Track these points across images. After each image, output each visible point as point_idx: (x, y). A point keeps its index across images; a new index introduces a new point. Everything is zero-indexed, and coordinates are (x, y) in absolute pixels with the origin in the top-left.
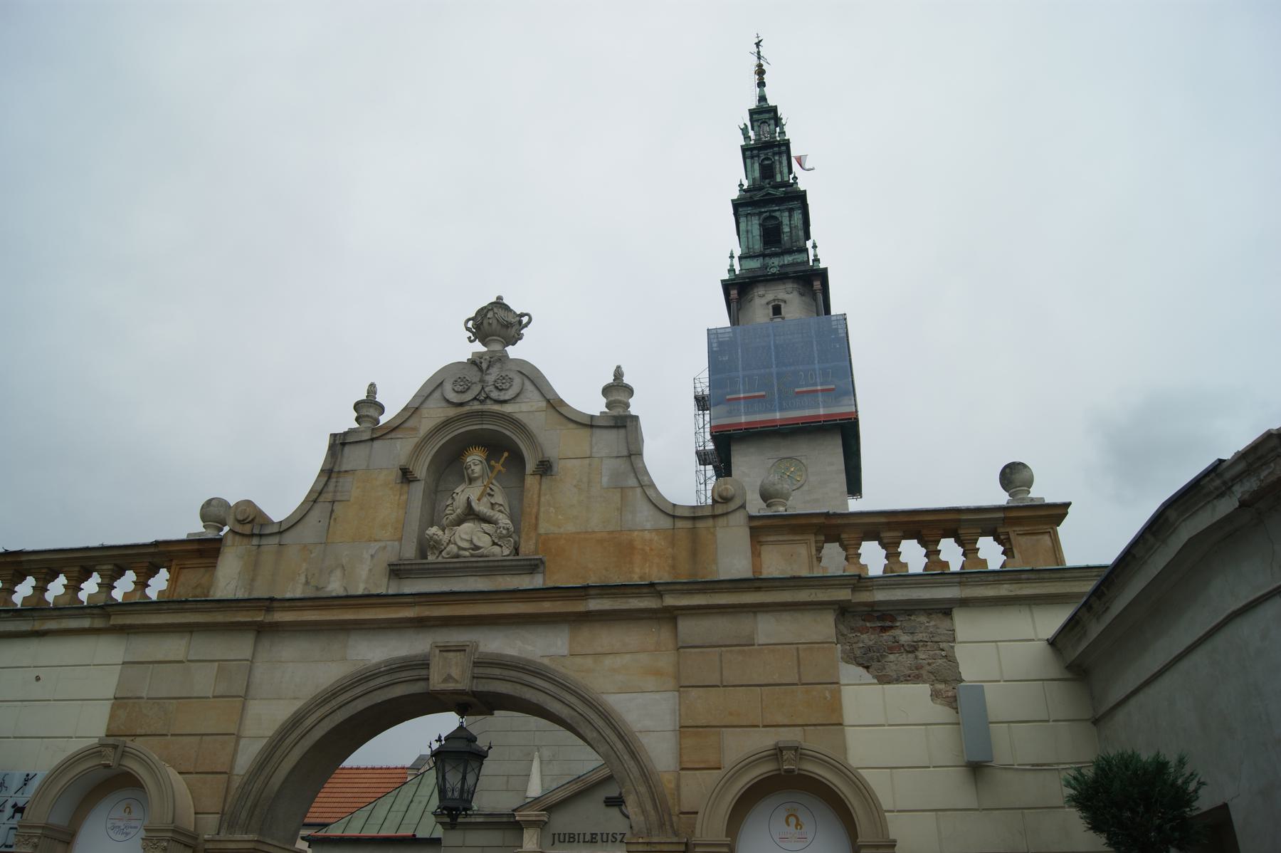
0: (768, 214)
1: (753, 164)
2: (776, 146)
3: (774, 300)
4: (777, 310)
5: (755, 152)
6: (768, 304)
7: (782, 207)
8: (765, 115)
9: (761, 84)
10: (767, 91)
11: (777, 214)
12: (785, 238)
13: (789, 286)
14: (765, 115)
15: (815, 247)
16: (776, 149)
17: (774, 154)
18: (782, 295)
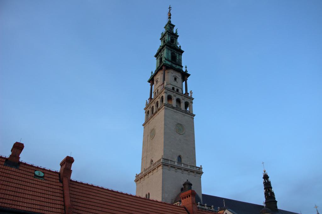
0: (173, 52)
1: (169, 36)
2: (175, 36)
3: (175, 76)
4: (175, 79)
5: (170, 34)
6: (173, 76)
7: (178, 53)
8: (170, 26)
9: (170, 18)
10: (171, 20)
11: (175, 53)
12: (177, 61)
13: (180, 74)
14: (170, 26)
15: (186, 67)
16: (175, 36)
17: (174, 37)
18: (177, 76)
